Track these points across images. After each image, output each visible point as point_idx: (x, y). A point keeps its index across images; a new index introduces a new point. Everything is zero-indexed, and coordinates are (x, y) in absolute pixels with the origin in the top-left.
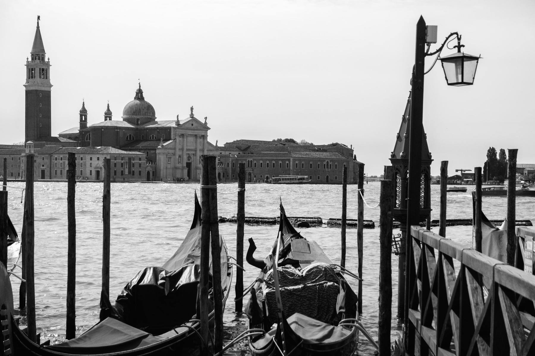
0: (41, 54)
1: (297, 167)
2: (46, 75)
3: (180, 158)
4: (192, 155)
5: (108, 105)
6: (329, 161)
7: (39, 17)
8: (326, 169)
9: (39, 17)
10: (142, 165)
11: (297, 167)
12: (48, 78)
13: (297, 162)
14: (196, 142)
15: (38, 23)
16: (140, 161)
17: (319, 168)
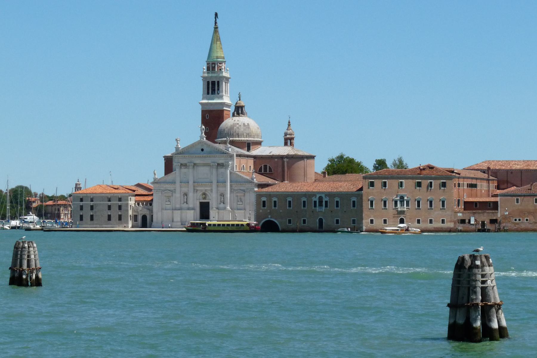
0: (211, 63)
1: (264, 206)
2: (218, 89)
3: (186, 195)
4: (209, 192)
5: (289, 123)
6: (323, 196)
7: (216, 15)
8: (318, 208)
9: (216, 15)
10: (123, 208)
11: (264, 206)
12: (220, 94)
13: (264, 199)
14: (212, 174)
15: (216, 23)
16: (120, 203)
17: (304, 206)
